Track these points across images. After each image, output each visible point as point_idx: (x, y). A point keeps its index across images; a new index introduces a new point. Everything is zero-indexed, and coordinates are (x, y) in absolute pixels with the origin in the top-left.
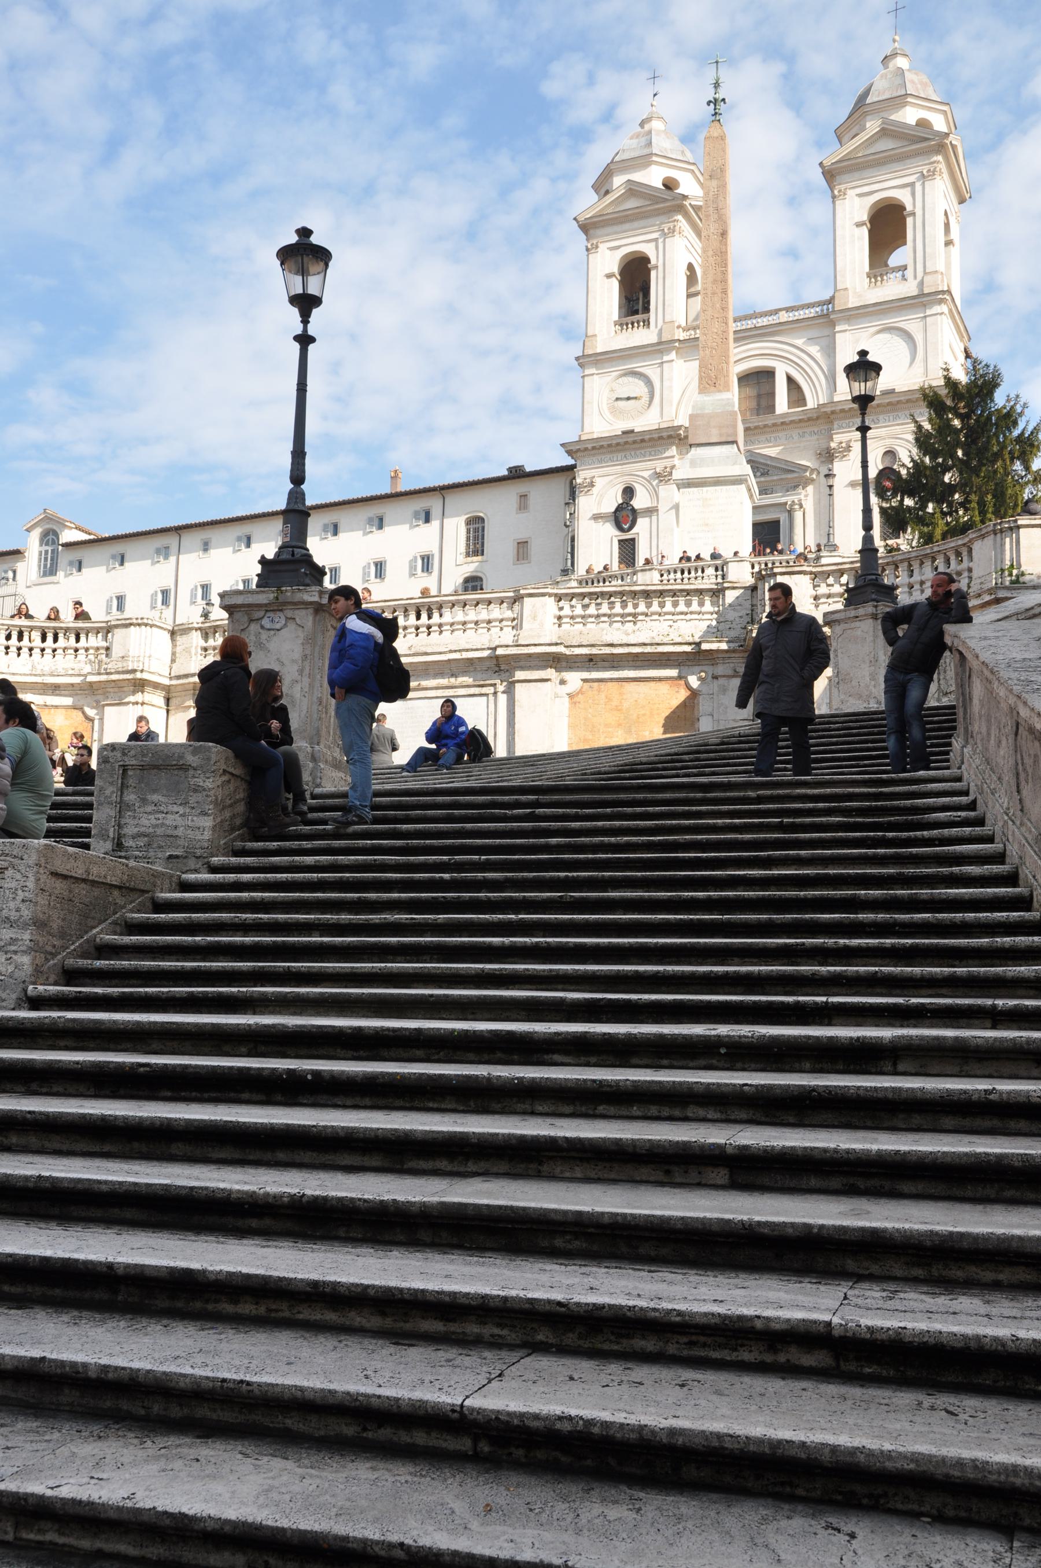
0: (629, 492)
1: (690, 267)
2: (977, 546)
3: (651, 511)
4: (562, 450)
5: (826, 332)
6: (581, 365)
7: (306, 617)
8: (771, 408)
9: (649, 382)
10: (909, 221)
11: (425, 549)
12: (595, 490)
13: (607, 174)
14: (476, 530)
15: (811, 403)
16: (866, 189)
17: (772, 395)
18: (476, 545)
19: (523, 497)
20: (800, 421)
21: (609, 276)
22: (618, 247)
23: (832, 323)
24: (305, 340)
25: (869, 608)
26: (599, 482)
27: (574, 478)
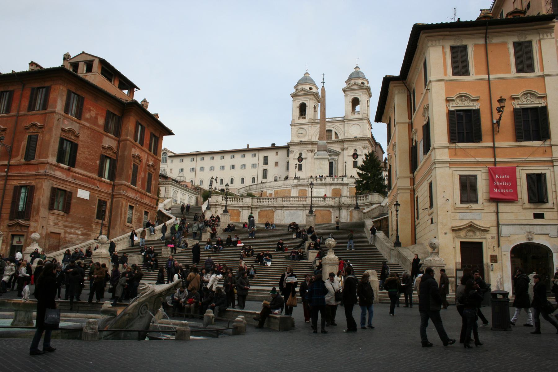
0: (301, 154)
1: (315, 106)
2: (369, 196)
3: (306, 158)
5: (343, 123)
7: (313, 216)
8: (331, 138)
10: (360, 102)
11: (254, 163)
12: (294, 153)
13: (297, 85)
14: (266, 159)
16: (351, 95)
17: (332, 135)
18: (266, 162)
19: (277, 153)
21: (297, 107)
22: (299, 101)
23: (344, 122)
24: (312, 191)
25: (356, 210)
26: (295, 152)
27: (289, 150)
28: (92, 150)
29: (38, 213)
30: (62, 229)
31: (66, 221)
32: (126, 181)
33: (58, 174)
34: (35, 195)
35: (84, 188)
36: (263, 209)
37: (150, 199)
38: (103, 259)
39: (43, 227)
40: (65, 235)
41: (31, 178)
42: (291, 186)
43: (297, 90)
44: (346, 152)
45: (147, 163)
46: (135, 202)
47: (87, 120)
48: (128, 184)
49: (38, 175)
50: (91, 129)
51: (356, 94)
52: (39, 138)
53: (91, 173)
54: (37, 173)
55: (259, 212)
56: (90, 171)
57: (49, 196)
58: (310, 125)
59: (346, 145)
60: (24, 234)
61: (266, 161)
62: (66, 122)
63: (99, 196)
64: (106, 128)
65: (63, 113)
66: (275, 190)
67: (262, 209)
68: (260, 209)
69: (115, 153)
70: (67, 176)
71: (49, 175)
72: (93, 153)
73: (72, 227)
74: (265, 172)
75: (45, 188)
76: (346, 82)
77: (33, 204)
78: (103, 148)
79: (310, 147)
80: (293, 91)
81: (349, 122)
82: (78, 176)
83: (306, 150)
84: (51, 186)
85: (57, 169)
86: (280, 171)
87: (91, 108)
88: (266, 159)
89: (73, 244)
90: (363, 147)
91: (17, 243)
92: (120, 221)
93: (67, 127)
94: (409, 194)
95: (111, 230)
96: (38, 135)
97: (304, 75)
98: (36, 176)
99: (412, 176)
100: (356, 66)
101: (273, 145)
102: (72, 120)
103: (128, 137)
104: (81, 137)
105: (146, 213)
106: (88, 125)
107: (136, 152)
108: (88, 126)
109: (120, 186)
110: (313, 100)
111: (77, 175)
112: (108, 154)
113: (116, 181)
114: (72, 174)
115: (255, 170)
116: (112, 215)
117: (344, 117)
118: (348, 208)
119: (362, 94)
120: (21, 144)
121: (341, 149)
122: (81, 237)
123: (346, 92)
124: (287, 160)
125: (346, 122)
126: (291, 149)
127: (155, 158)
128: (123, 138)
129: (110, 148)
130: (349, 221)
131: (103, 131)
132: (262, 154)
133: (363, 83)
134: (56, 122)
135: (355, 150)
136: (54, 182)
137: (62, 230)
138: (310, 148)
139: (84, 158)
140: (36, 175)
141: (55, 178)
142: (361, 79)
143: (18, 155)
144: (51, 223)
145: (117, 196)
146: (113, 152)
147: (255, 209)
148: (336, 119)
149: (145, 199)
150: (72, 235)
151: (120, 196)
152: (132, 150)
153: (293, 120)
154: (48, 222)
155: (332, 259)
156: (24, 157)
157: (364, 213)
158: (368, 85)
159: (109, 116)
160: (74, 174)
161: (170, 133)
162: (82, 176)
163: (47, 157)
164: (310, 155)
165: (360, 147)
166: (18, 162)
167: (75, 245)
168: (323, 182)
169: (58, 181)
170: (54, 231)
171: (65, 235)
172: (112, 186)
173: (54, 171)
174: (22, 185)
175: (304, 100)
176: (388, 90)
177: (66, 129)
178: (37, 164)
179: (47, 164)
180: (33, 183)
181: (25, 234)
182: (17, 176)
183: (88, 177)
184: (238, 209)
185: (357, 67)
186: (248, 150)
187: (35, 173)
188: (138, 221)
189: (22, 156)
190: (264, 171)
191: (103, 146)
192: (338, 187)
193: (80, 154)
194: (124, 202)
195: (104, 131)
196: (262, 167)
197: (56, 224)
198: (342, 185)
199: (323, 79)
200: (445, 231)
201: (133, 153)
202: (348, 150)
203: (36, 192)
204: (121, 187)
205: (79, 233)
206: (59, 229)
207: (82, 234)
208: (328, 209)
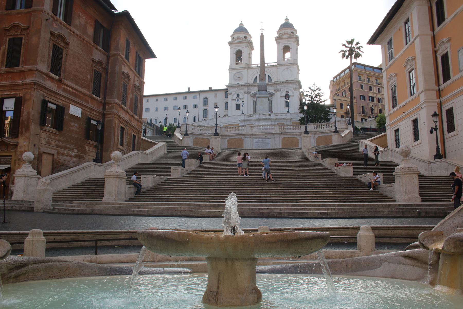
0: (238, 96)
1: (249, 53)
4: (226, 87)
5: (275, 68)
6: (229, 70)
9: (242, 74)
10: (291, 50)
12: (232, 94)
15: (273, 81)
19: (216, 94)
20: (271, 84)
21: (234, 54)
23: (277, 67)
25: (337, 134)
26: (233, 93)
27: (227, 91)
28: (83, 62)
29: (28, 129)
30: (54, 149)
31: (59, 140)
32: (118, 99)
33: (49, 84)
34: (23, 108)
35: (76, 104)
36: (232, 137)
37: (137, 122)
38: (120, 179)
39: (35, 145)
40: (58, 156)
41: (16, 88)
42: (239, 121)
43: (233, 38)
44: (278, 95)
45: (134, 84)
46: (125, 123)
47: (76, 27)
48: (120, 103)
49: (26, 84)
50: (81, 38)
51: (286, 43)
53: (83, 88)
54: (25, 82)
55: (228, 141)
56: (81, 86)
57: (40, 110)
58: (246, 70)
59: (279, 87)
61: (206, 102)
62: (55, 26)
63: (92, 115)
64: (95, 39)
65: (52, 14)
66: (223, 125)
67: (230, 137)
68: (229, 137)
69: (104, 69)
70: (59, 87)
71: (39, 85)
72: (84, 66)
73: (66, 148)
74: (205, 112)
75: (35, 100)
76: (278, 32)
77: (21, 118)
78: (93, 61)
79: (246, 89)
80: (230, 39)
81: (281, 67)
82: (69, 90)
83: (243, 92)
84: (42, 98)
85: (47, 78)
86: (220, 111)
87: (80, 15)
88: (206, 100)
89: (67, 168)
90: (294, 89)
92: (114, 142)
93: (56, 31)
94: (437, 107)
95: (104, 153)
97: (239, 25)
98: (23, 85)
99: (438, 89)
100: (286, 18)
101: (210, 88)
102: (62, 24)
103: (119, 52)
104: (71, 47)
105: (134, 136)
106: (78, 33)
107: (125, 70)
108: (78, 34)
109: (113, 105)
110: (248, 47)
111: (68, 88)
112: (98, 69)
113: (107, 100)
114: (63, 86)
115: (196, 110)
116: (105, 135)
117: (276, 63)
118: (315, 135)
119: (292, 42)
121: (275, 91)
122: (74, 159)
123: (278, 41)
124: (225, 100)
125: (278, 67)
126: (229, 91)
127: (140, 79)
128: (111, 53)
129: (99, 62)
130: (316, 146)
131: (93, 42)
132: (203, 96)
133: (292, 32)
134: (44, 23)
135: (287, 91)
136: (44, 94)
137: (54, 151)
138: (247, 90)
139: (76, 71)
140: (22, 85)
141: (45, 88)
142: (291, 29)
144: (43, 142)
145: (109, 116)
146: (103, 68)
147: (224, 138)
148: (269, 64)
149: (133, 122)
150: (65, 157)
151: (112, 115)
152: (122, 68)
153: (231, 65)
154: (40, 140)
155: (411, 168)
157: (342, 137)
158: (297, 35)
159: (98, 26)
160: (66, 87)
161: (152, 55)
162: (73, 91)
163: (35, 63)
164: (246, 95)
165: (292, 89)
167: (69, 168)
168: (270, 117)
169: (49, 93)
170: (46, 151)
171: (58, 156)
172: (102, 105)
173: (44, 81)
174: (5, 96)
175: (240, 47)
176: (403, 2)
177: (55, 33)
178: (24, 72)
179: (36, 71)
180: (20, 93)
181: (13, 154)
183: (80, 92)
184: (208, 137)
185: (287, 19)
186: (189, 92)
187: (20, 82)
188: (128, 144)
190: (205, 111)
191: (93, 59)
193: (70, 64)
194: (117, 122)
195: (94, 42)
196: (202, 107)
197: (49, 143)
198: (286, 119)
199: (262, 26)
201: (123, 71)
202: (281, 91)
203: (24, 104)
204: (113, 106)
205: (73, 154)
206: (52, 148)
207: (76, 156)
208: (295, 136)
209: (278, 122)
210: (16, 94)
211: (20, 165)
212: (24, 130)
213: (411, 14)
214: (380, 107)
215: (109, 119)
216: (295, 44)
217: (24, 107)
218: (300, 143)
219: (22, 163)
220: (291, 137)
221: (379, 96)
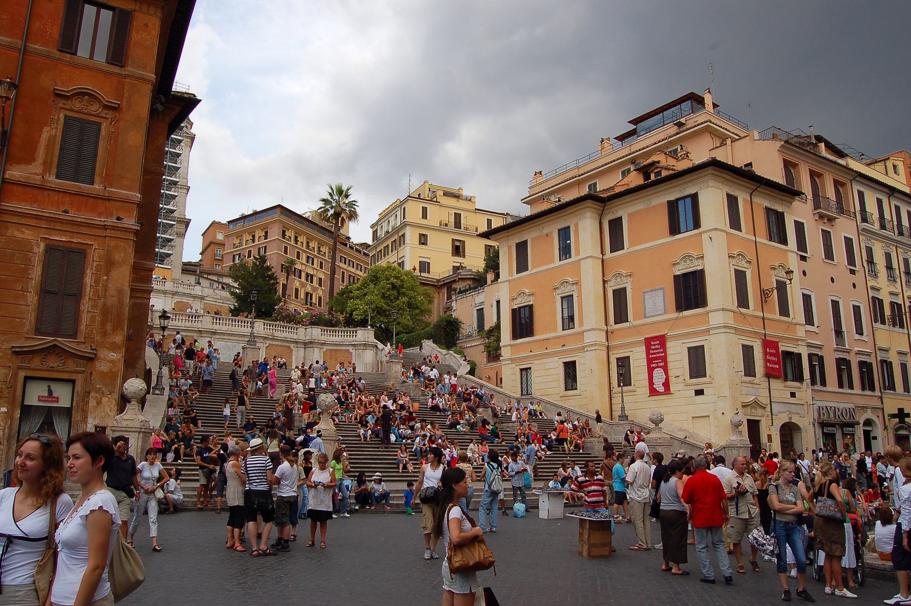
41: (84, 230)
52: (103, 132)
60: (73, 377)
91: (39, 400)
96: (100, 124)
98: (106, 229)
120: (41, 133)
143: (34, 160)
156: (54, 170)
166: (37, 180)
182: (37, 217)
189: (45, 163)
192: (185, 300)
198: (195, 297)
200: (737, 407)
208: (287, 344)
209: (178, 300)
210: (87, 244)
211: (99, 403)
212: (109, 327)
213: (576, 225)
214: (309, 289)
215: (139, 301)
216: (188, 148)
217: (107, 275)
218: (294, 357)
219: (105, 400)
220: (281, 345)
221: (311, 272)
